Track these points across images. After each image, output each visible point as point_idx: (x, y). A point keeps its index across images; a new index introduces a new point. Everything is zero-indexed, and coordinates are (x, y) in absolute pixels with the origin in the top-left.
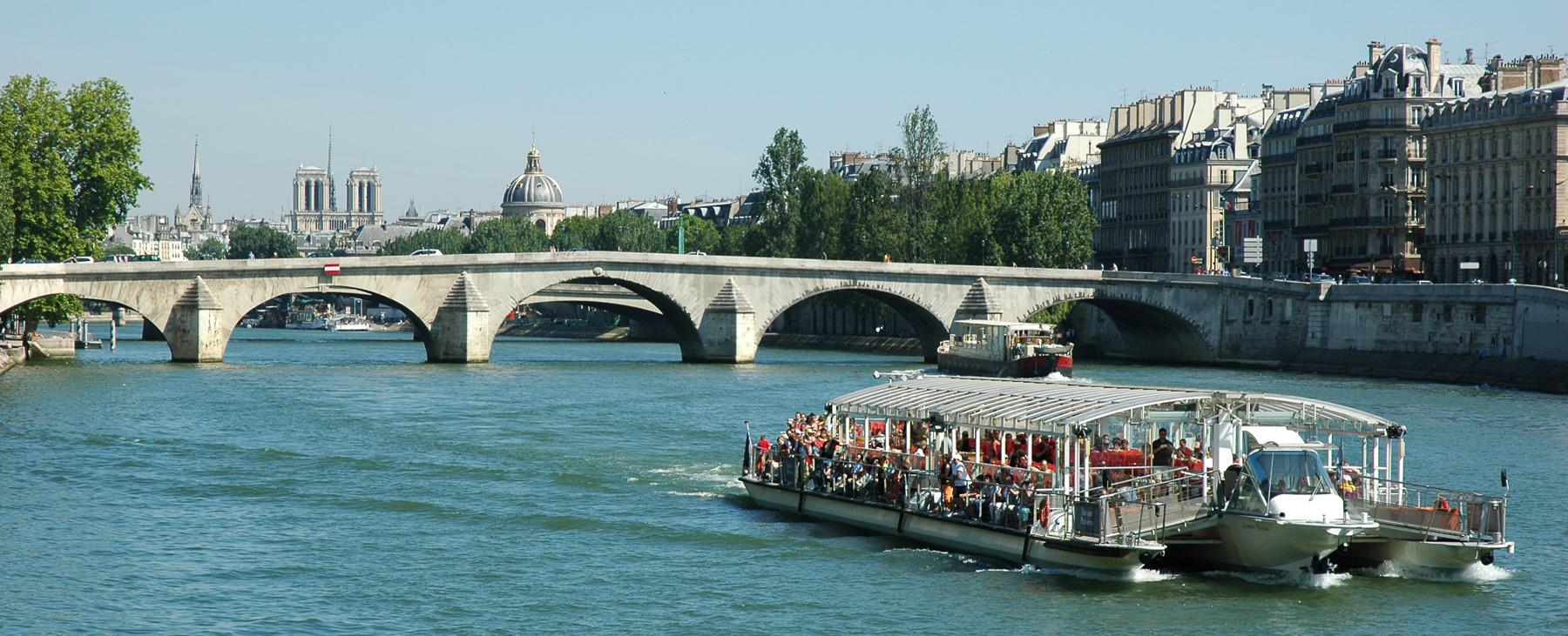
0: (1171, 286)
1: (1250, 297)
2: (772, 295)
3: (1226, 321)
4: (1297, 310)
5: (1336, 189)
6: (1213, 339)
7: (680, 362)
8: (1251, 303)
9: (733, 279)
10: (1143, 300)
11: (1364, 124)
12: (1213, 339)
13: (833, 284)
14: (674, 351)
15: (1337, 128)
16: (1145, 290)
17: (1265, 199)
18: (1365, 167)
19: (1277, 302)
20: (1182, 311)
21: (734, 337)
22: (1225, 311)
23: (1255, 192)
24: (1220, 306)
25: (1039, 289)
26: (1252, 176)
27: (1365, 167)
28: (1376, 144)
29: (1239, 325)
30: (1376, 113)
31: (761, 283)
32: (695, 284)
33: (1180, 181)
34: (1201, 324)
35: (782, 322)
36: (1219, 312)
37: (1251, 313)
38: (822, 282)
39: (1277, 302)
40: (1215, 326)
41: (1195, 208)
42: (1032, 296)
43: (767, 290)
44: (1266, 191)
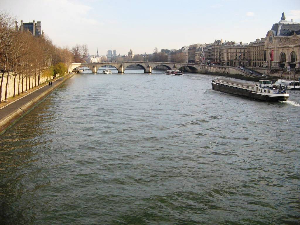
4: (207, 68)
5: (212, 55)
7: (143, 73)
9: (149, 64)
11: (215, 48)
12: (199, 70)
13: (160, 64)
14: (143, 71)
15: (212, 48)
18: (215, 52)
19: (205, 67)
20: (196, 67)
25: (181, 65)
27: (215, 52)
29: (201, 69)
30: (216, 47)
39: (205, 67)
42: (180, 65)
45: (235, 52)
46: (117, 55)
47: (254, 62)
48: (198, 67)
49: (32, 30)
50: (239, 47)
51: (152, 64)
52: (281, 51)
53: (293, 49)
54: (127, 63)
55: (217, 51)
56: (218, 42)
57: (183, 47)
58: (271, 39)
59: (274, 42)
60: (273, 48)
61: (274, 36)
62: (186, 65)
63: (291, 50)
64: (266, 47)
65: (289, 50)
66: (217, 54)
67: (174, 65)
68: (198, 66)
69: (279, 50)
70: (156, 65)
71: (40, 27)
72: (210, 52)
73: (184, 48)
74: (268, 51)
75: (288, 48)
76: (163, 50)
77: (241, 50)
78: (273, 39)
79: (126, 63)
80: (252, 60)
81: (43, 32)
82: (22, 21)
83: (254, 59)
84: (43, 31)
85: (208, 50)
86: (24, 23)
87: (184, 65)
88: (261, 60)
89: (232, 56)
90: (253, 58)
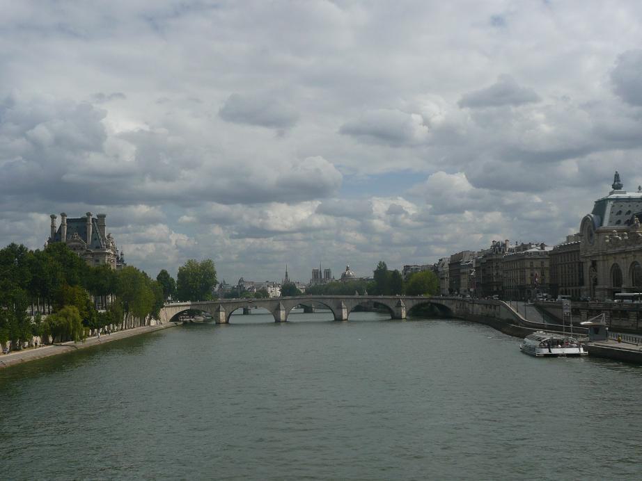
3: (457, 308)
12: (454, 312)
15: (487, 261)
20: (447, 305)
28: (494, 265)
30: (494, 257)
40: (455, 308)
45: (529, 267)
47: (564, 289)
48: (452, 304)
49: (84, 234)
50: (538, 257)
52: (612, 262)
53: (635, 256)
55: (497, 266)
56: (498, 247)
58: (591, 235)
59: (596, 243)
60: (595, 256)
61: (594, 229)
63: (631, 259)
64: (582, 254)
65: (626, 258)
66: (497, 274)
68: (451, 302)
69: (608, 260)
72: (484, 270)
74: (586, 262)
75: (624, 255)
77: (542, 262)
78: (595, 235)
79: (290, 301)
80: (560, 285)
81: (111, 235)
82: (63, 215)
83: (567, 282)
85: (482, 263)
86: (67, 220)
87: (420, 301)
88: (572, 284)
89: (523, 278)
90: (560, 279)
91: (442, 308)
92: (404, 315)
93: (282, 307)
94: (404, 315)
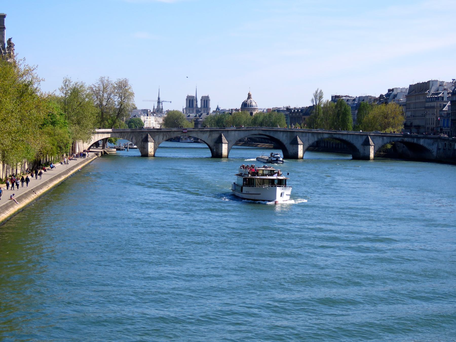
0: (423, 138)
1: (445, 142)
2: (308, 140)
3: (439, 149)
6: (435, 154)
8: (445, 143)
10: (415, 142)
12: (435, 154)
16: (415, 139)
17: (452, 113)
20: (426, 146)
21: (298, 152)
22: (438, 146)
23: (449, 111)
24: (437, 145)
25: (385, 138)
26: (448, 106)
31: (306, 136)
32: (286, 136)
33: (428, 107)
34: (431, 149)
35: (315, 143)
36: (436, 146)
37: (445, 147)
38: (323, 135)
41: (432, 114)
43: (307, 138)
44: (452, 110)
46: (213, 108)
51: (304, 135)
54: (237, 132)
57: (393, 90)
62: (400, 139)
67: (364, 137)
70: (316, 139)
71: (4, 28)
73: (395, 92)
76: (335, 98)
79: (233, 133)
81: (12, 41)
84: (10, 40)
91: (422, 149)
92: (372, 155)
93: (224, 140)
94: (372, 155)
